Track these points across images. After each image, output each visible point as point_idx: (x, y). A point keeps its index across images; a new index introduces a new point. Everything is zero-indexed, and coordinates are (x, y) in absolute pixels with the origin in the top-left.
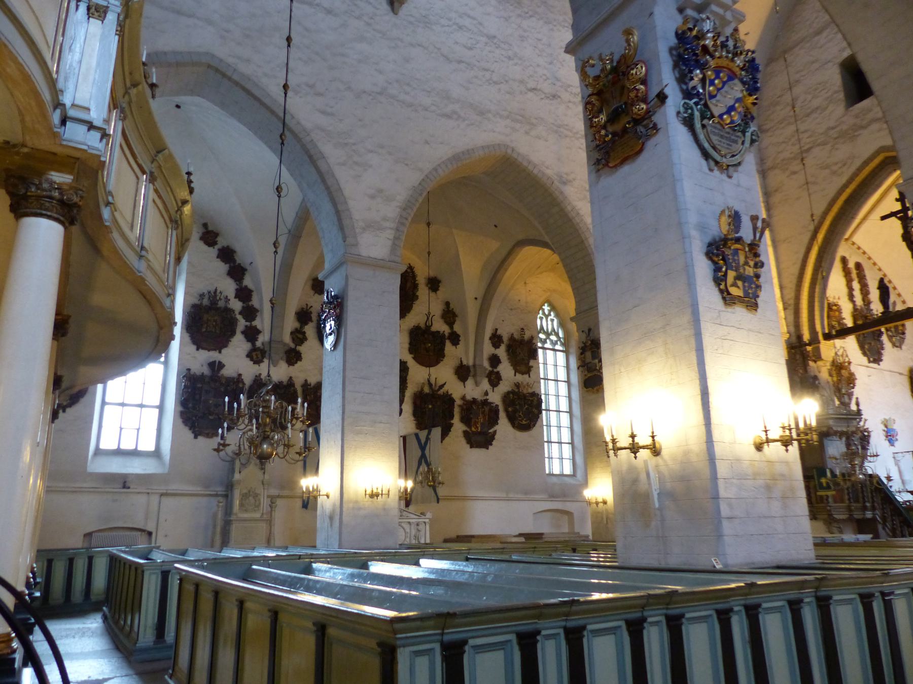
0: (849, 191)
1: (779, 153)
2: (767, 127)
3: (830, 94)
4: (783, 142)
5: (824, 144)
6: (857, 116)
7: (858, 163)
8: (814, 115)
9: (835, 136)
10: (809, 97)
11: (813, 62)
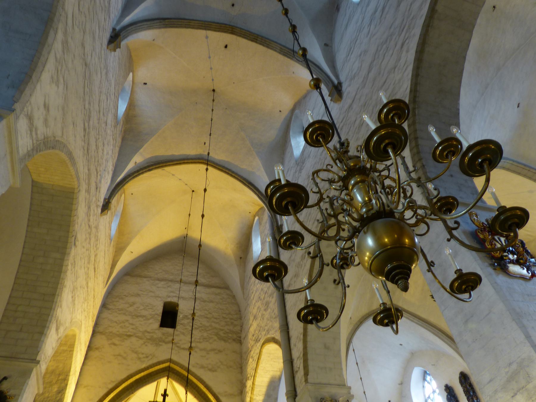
0: (142, 374)
1: (110, 326)
2: (110, 307)
3: (153, 313)
4: (116, 322)
5: (141, 338)
6: (163, 334)
7: (155, 361)
8: (141, 319)
9: (148, 337)
10: (142, 308)
11: (151, 292)
